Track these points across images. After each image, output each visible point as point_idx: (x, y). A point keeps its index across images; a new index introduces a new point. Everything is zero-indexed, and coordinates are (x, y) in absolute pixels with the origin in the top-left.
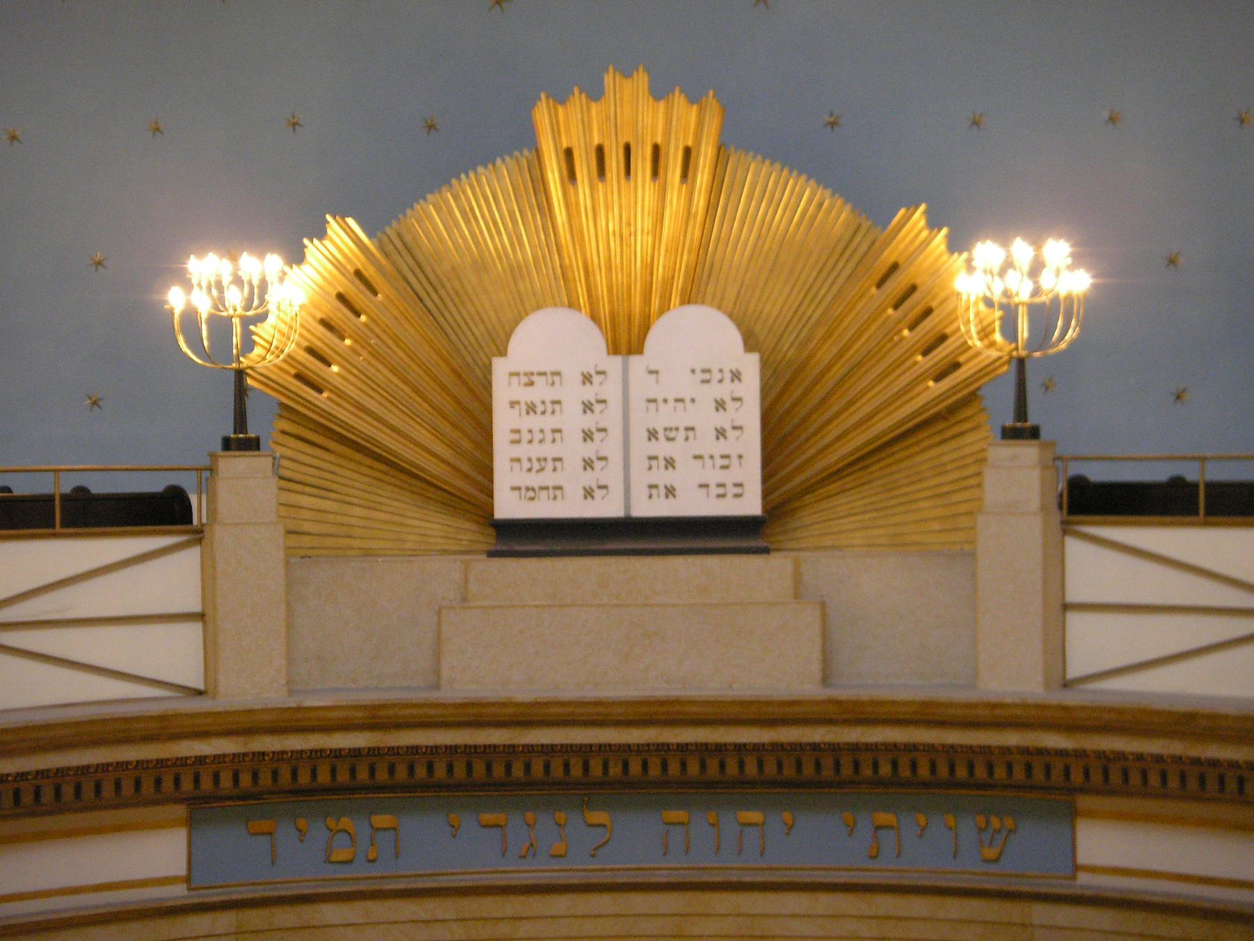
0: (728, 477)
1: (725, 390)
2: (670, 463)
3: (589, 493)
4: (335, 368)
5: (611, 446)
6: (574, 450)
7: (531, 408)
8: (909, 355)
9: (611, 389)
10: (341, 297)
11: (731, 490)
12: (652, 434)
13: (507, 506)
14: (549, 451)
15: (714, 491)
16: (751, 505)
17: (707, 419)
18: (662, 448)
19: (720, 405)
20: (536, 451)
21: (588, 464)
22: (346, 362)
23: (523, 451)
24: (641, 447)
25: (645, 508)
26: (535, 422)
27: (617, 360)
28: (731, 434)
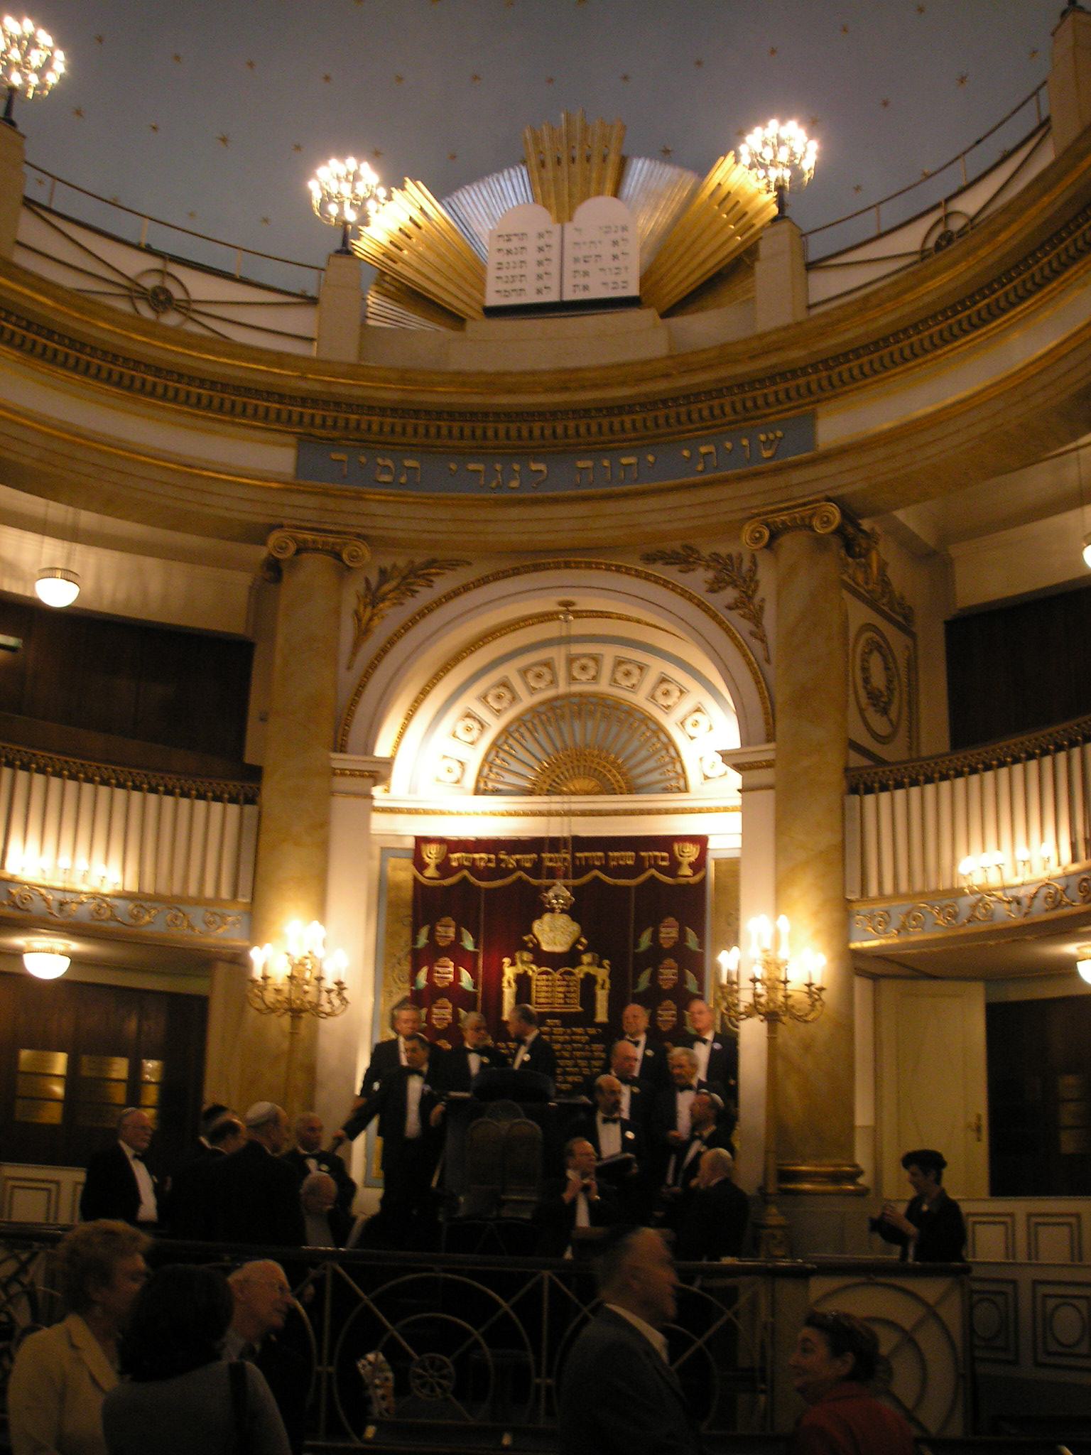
0: (619, 279)
1: (617, 236)
2: (586, 274)
3: (539, 292)
4: (405, 252)
5: (554, 268)
6: (531, 270)
7: (509, 252)
8: (728, 223)
9: (554, 240)
10: (411, 219)
11: (621, 284)
12: (576, 260)
13: (493, 300)
14: (518, 272)
15: (611, 285)
16: (633, 290)
17: (607, 250)
18: (581, 267)
19: (615, 243)
20: (511, 272)
21: (540, 277)
22: (411, 249)
23: (501, 273)
24: (569, 266)
25: (569, 296)
26: (511, 258)
27: (558, 226)
28: (621, 257)
